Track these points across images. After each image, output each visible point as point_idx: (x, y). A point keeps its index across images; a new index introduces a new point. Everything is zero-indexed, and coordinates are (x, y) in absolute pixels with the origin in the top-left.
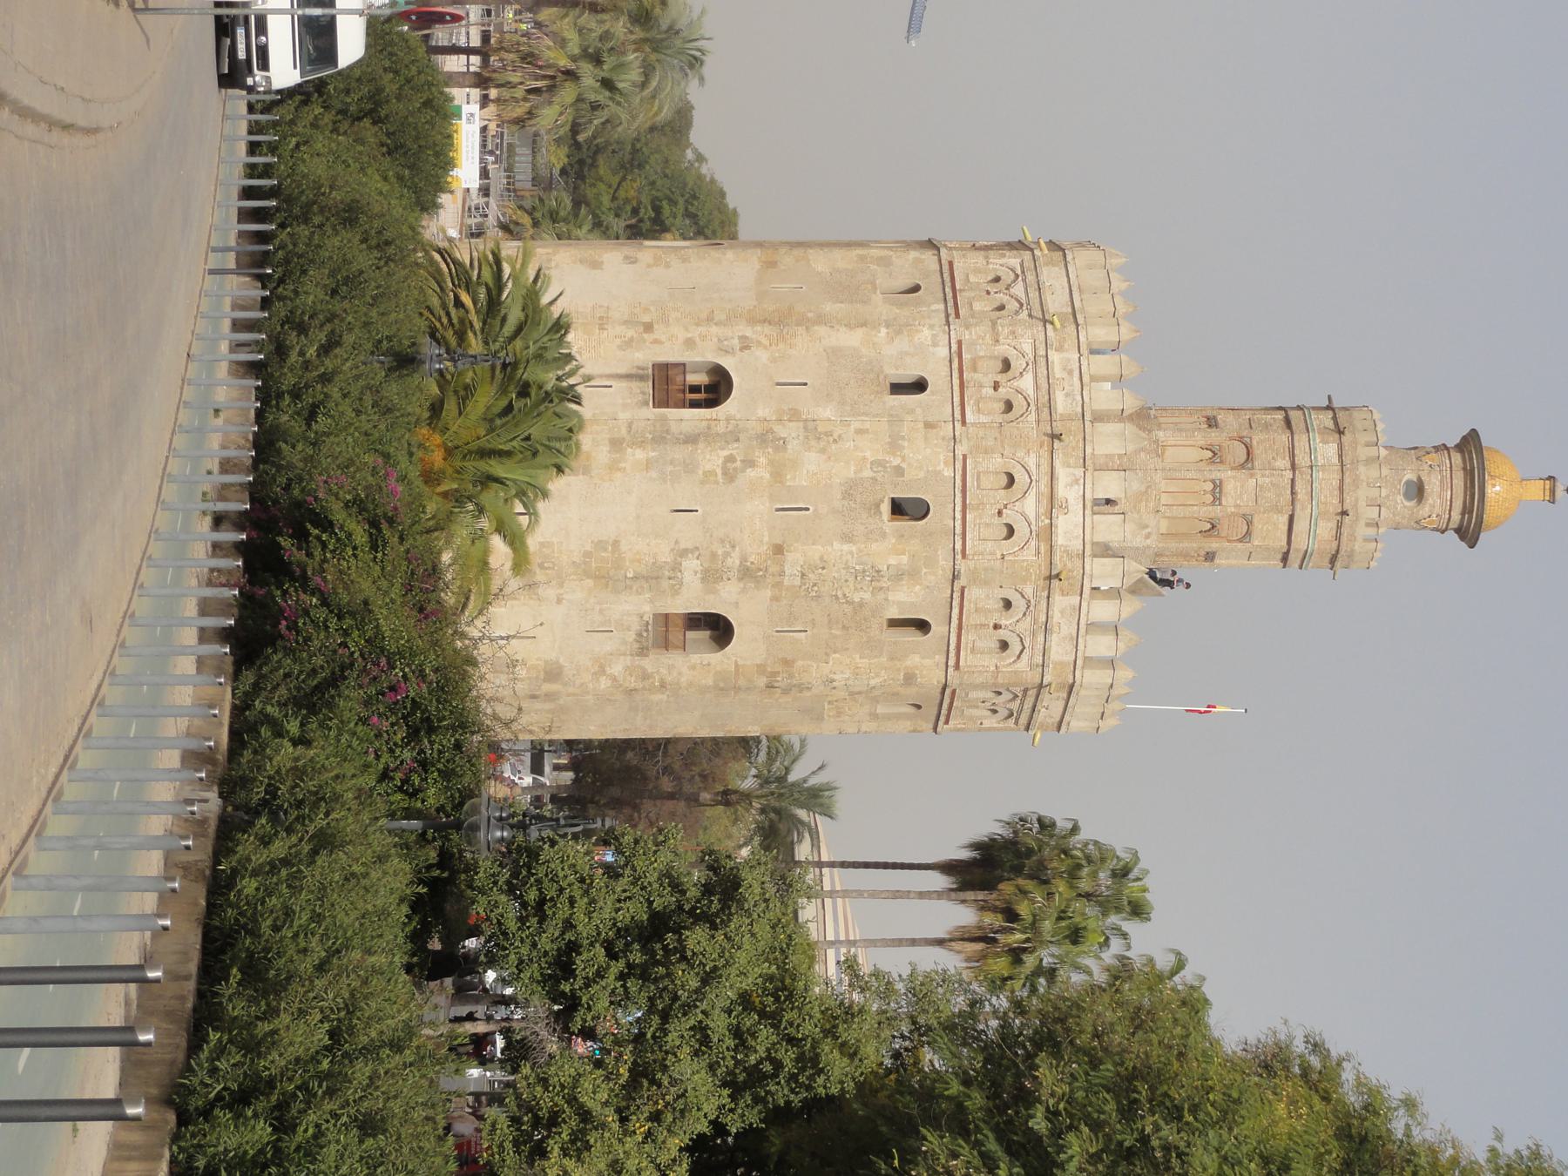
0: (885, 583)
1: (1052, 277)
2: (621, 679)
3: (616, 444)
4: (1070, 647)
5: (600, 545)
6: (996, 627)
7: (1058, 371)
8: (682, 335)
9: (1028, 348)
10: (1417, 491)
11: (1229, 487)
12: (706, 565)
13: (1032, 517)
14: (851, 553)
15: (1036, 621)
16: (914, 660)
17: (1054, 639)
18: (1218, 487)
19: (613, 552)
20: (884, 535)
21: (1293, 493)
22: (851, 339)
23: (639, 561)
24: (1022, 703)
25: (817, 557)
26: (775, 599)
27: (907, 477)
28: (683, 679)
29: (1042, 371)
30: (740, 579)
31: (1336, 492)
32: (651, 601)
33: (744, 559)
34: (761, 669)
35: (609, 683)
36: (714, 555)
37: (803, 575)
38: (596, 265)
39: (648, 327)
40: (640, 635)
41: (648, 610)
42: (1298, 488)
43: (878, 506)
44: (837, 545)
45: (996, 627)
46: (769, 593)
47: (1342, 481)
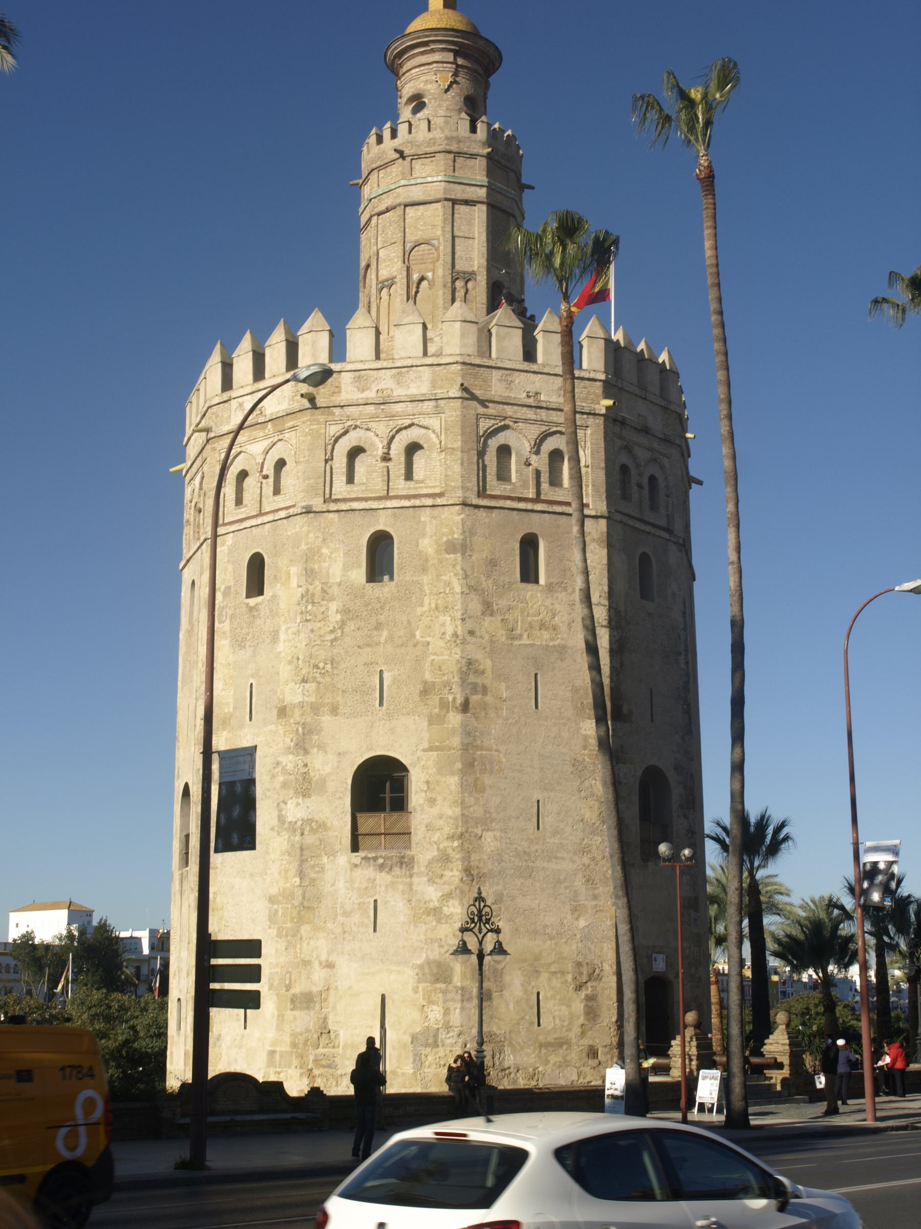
0: (317, 586)
2: (447, 889)
4: (412, 373)
6: (386, 458)
11: (384, 273)
12: (291, 792)
13: (266, 443)
14: (287, 629)
15: (373, 417)
16: (427, 545)
17: (400, 392)
19: (278, 902)
20: (274, 597)
21: (388, 210)
23: (286, 871)
24: (526, 421)
25: (288, 668)
26: (334, 711)
27: (232, 584)
28: (449, 812)
30: (306, 752)
31: (389, 169)
32: (333, 854)
33: (288, 750)
34: (433, 720)
35: (451, 902)
36: (285, 785)
37: (304, 681)
40: (381, 867)
41: (345, 857)
42: (382, 207)
43: (251, 609)
44: (281, 647)
45: (386, 458)
46: (326, 719)
47: (379, 168)
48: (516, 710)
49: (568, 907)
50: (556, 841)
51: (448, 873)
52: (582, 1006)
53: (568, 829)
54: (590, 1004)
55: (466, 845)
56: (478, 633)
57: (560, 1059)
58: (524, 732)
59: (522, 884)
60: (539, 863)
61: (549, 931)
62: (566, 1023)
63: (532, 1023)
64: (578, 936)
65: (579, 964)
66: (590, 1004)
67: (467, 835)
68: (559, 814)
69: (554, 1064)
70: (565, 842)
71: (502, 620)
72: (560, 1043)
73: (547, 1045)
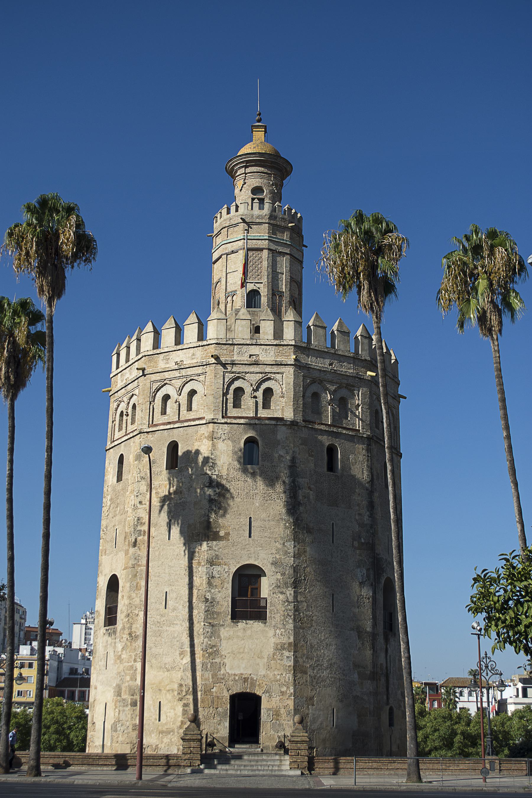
24: (175, 378)
41: (103, 630)
48: (159, 542)
49: (178, 652)
50: (174, 614)
51: (124, 636)
52: (181, 709)
53: (181, 607)
54: (186, 709)
55: (131, 620)
56: (143, 503)
57: (169, 740)
58: (162, 554)
59: (155, 640)
60: (165, 628)
61: (167, 666)
62: (172, 720)
63: (156, 719)
64: (182, 669)
65: (181, 685)
66: (186, 709)
67: (131, 614)
68: (176, 598)
69: (166, 743)
70: (178, 614)
71: (156, 493)
72: (169, 732)
73: (161, 732)
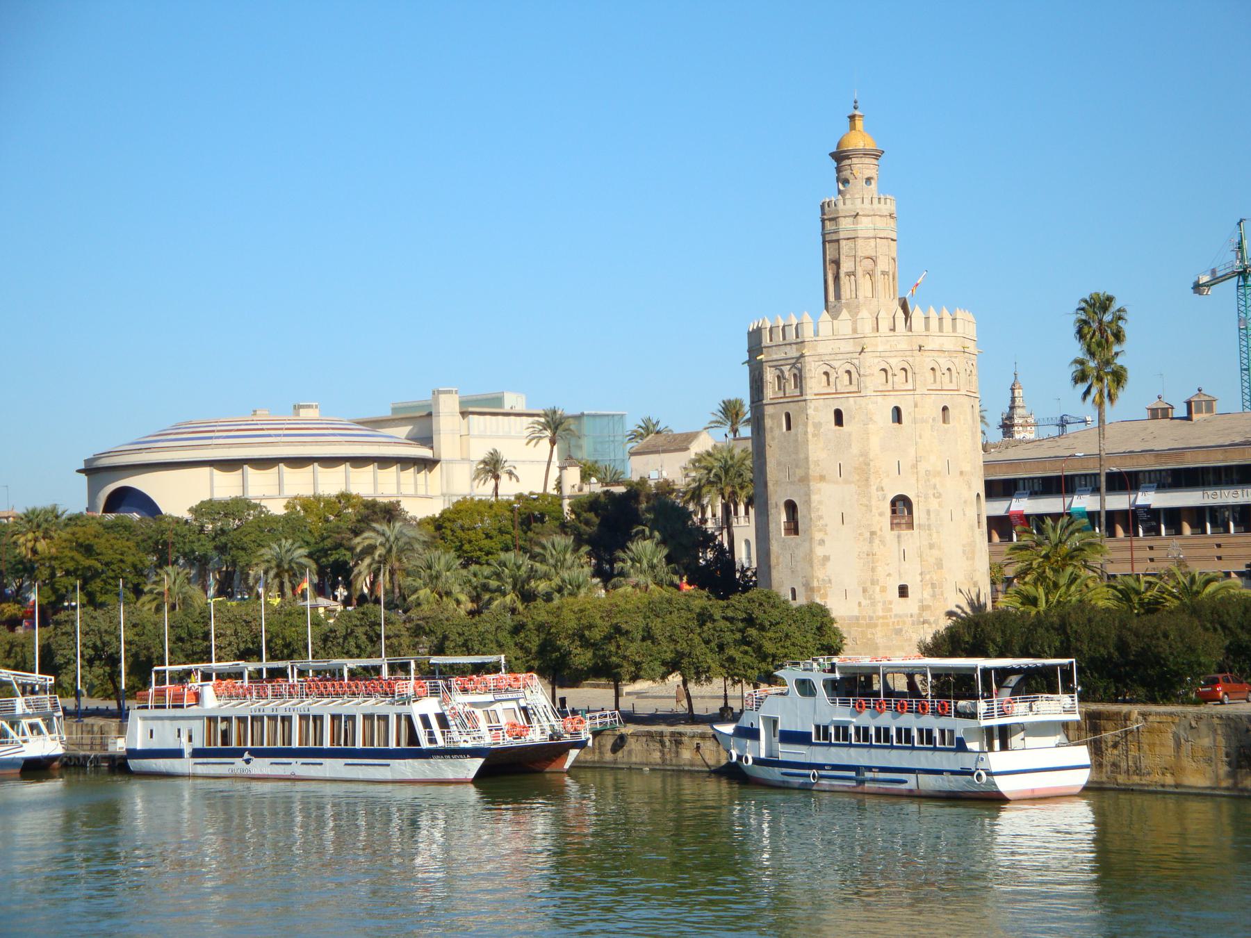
1: (823, 348)
3: (931, 546)
5: (964, 552)
7: (888, 348)
8: (877, 517)
9: (876, 360)
10: (868, 180)
18: (883, 273)
22: (875, 443)
29: (887, 354)
38: (826, 559)
39: (873, 533)
